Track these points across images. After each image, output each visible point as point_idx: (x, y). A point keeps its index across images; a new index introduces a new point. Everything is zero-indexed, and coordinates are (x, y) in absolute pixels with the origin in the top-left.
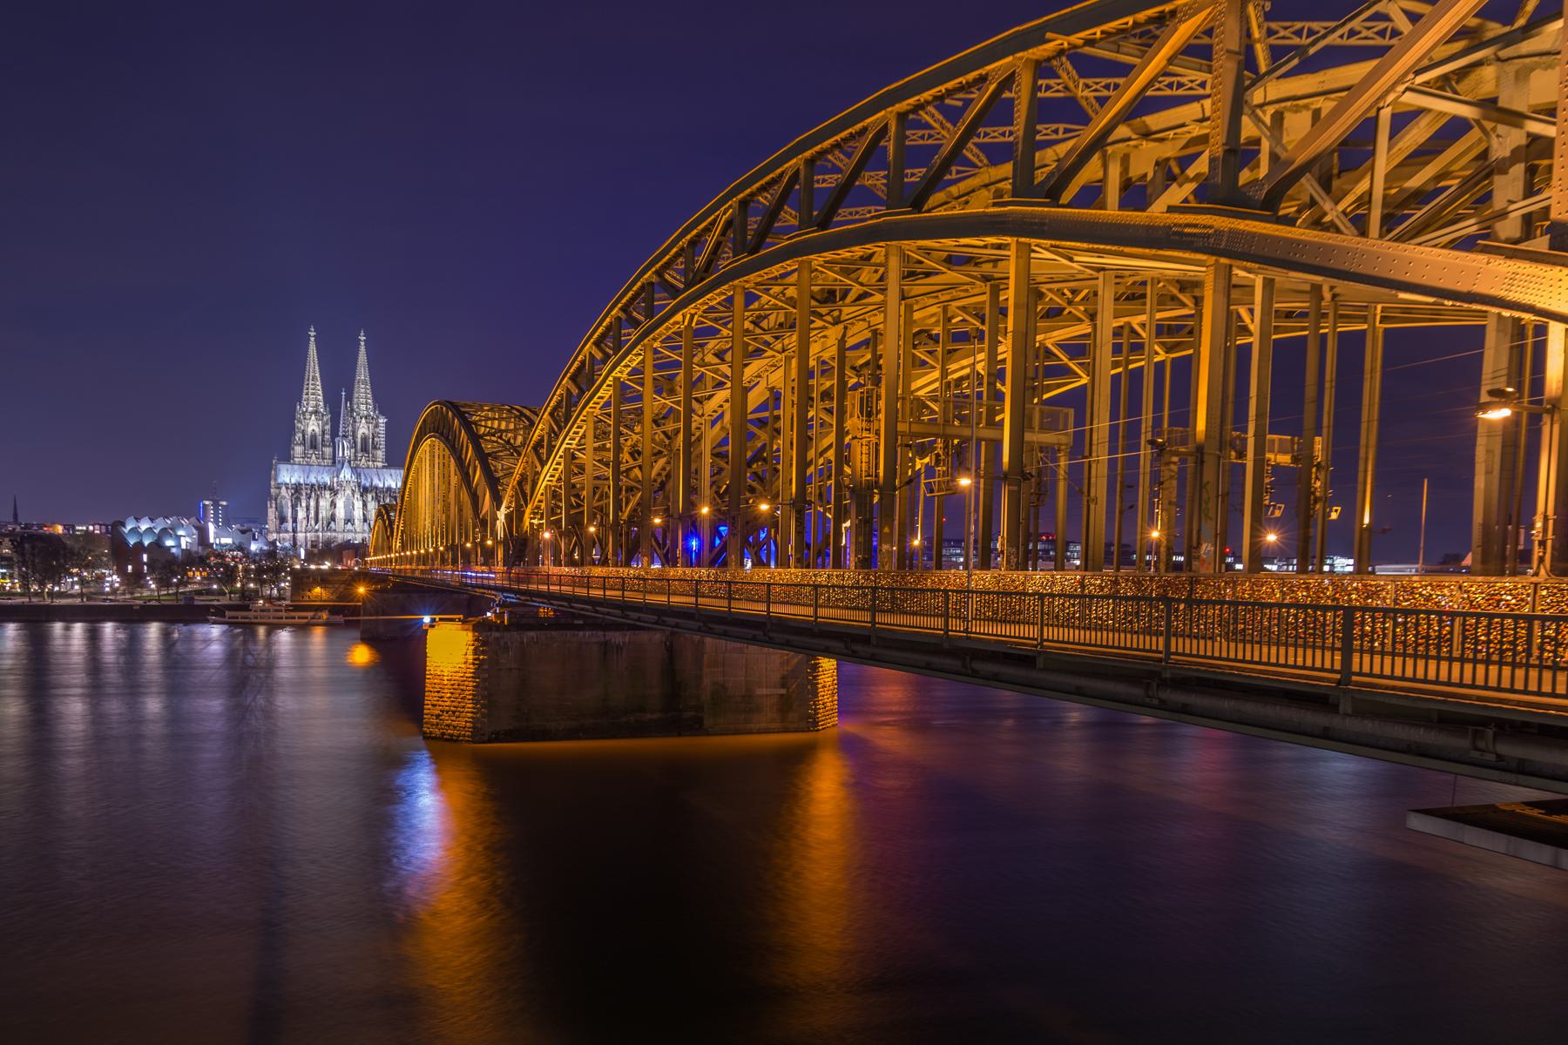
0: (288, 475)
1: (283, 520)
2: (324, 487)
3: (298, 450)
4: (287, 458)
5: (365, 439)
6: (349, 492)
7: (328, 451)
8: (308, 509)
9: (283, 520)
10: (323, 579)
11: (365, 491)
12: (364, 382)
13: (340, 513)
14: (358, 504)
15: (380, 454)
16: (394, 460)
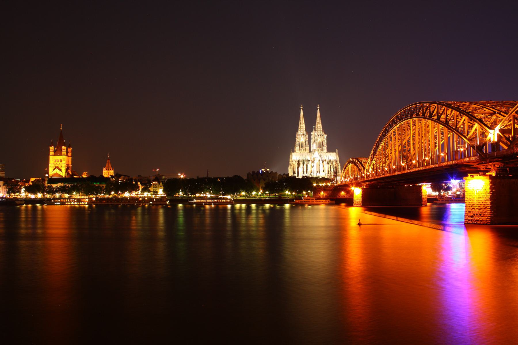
0: (295, 157)
1: (294, 173)
2: (308, 161)
3: (297, 148)
4: (293, 151)
5: (320, 144)
6: (318, 161)
7: (308, 148)
8: (303, 168)
9: (294, 173)
10: (325, 189)
11: (323, 161)
12: (319, 122)
13: (315, 169)
14: (321, 165)
15: (325, 148)
16: (330, 150)
